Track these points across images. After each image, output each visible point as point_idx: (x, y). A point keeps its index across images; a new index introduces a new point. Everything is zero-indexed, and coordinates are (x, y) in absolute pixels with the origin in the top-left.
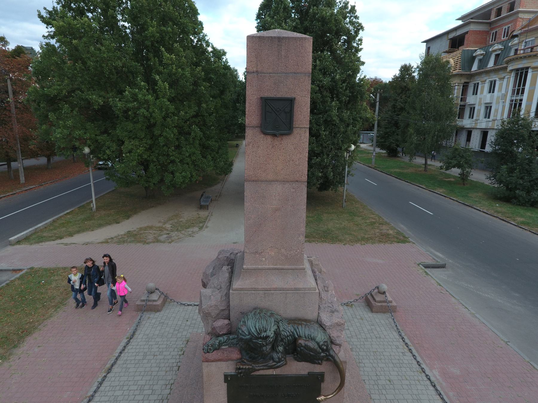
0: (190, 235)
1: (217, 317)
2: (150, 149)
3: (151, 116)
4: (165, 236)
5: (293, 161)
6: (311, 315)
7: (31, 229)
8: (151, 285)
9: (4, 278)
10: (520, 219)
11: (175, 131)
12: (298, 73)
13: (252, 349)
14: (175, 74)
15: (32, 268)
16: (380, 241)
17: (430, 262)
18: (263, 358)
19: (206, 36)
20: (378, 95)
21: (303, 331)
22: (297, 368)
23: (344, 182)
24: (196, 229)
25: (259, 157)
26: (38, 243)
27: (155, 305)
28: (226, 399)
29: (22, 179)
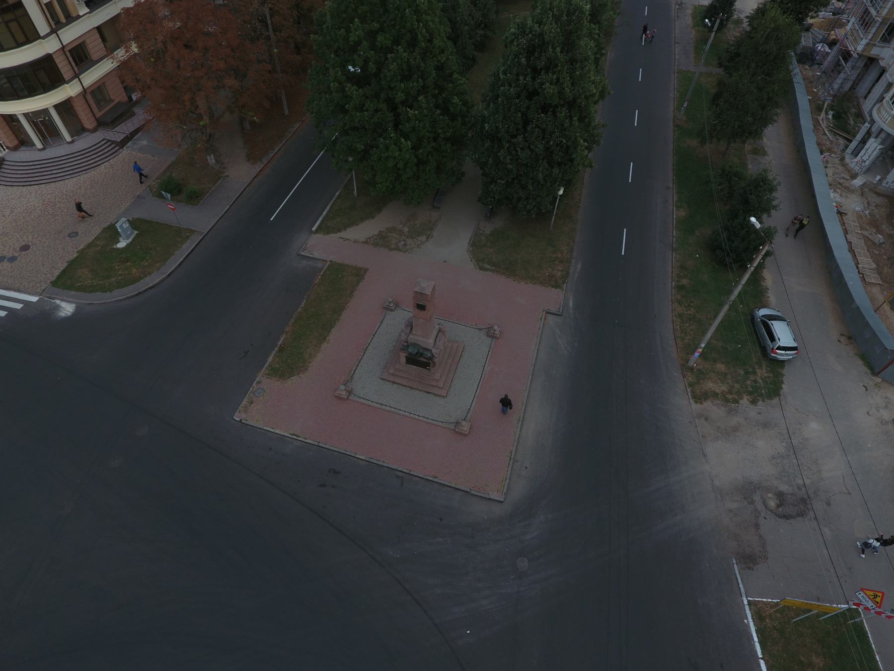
0: (419, 246)
4: (402, 243)
6: (430, 348)
7: (321, 219)
8: (390, 300)
9: (320, 265)
10: (685, 282)
11: (415, 169)
13: (410, 354)
15: (331, 261)
16: (541, 283)
17: (553, 310)
20: (718, 21)
21: (425, 352)
22: (422, 359)
24: (424, 238)
26: (328, 233)
29: (286, 112)
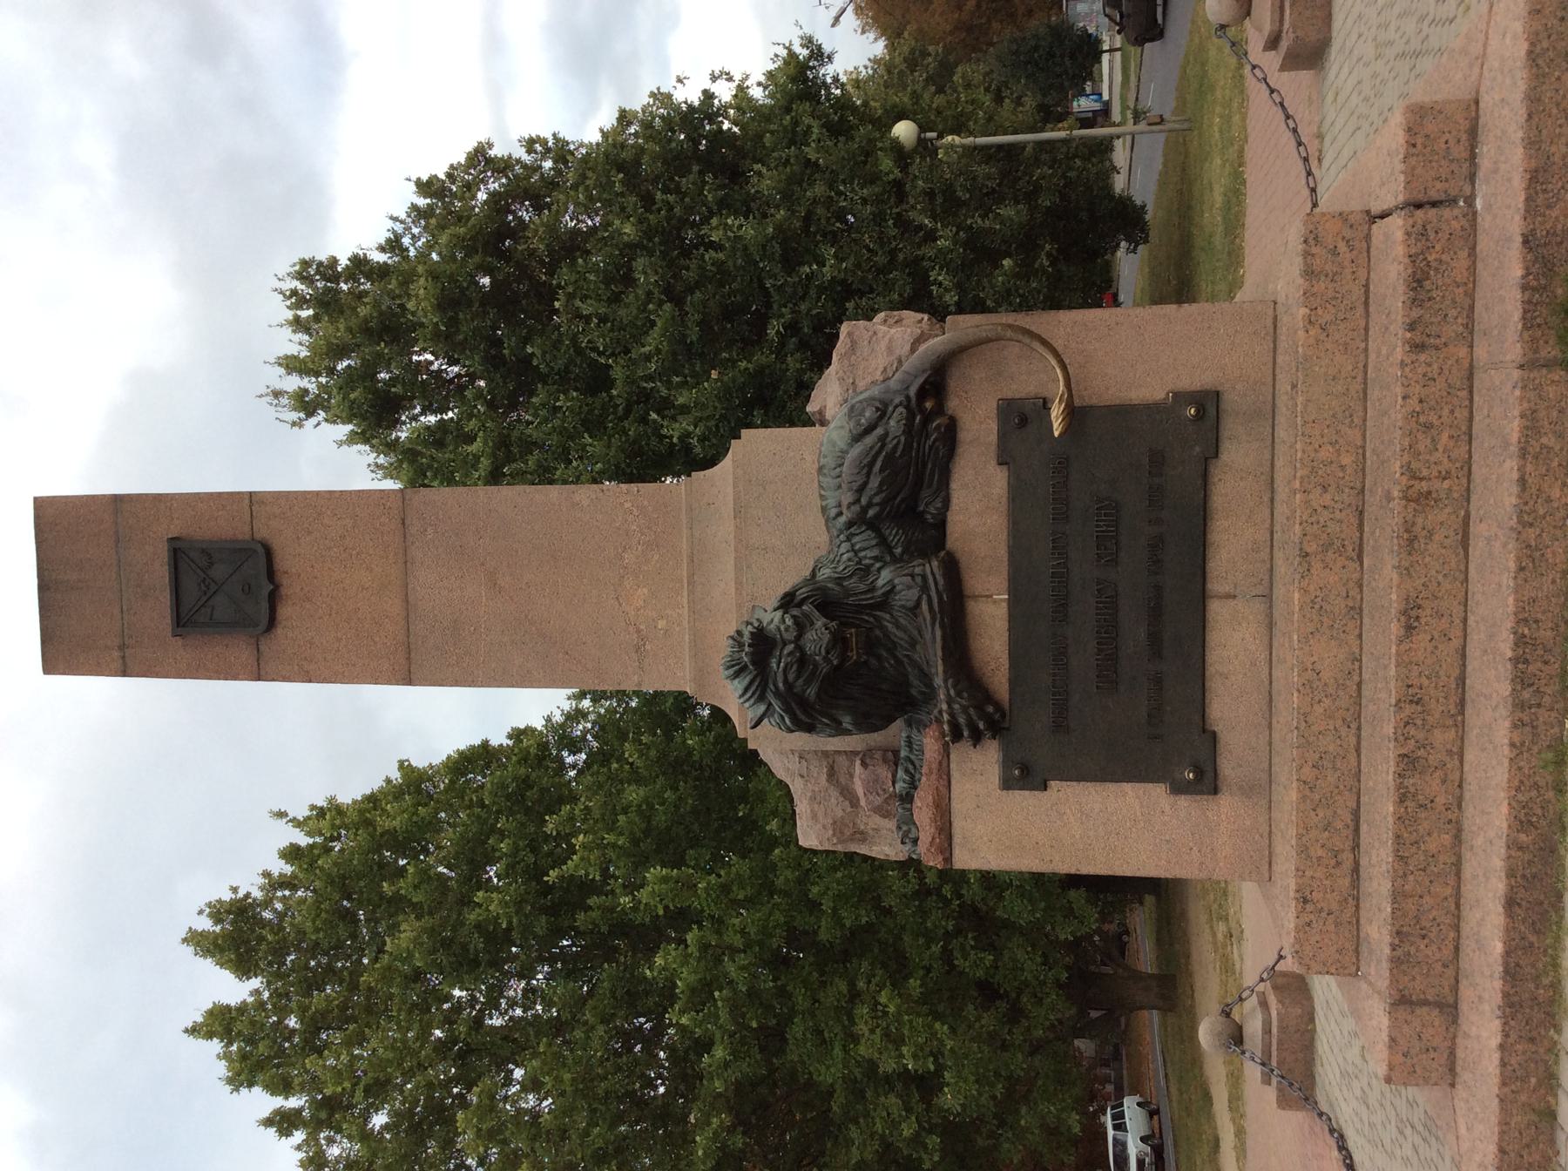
1: (848, 794)
2: (897, 969)
3: (761, 944)
5: (343, 537)
12: (117, 532)
14: (635, 842)
18: (913, 644)
19: (548, 719)
23: (1064, 141)
25: (339, 640)
27: (1282, 1029)
28: (1127, 787)
